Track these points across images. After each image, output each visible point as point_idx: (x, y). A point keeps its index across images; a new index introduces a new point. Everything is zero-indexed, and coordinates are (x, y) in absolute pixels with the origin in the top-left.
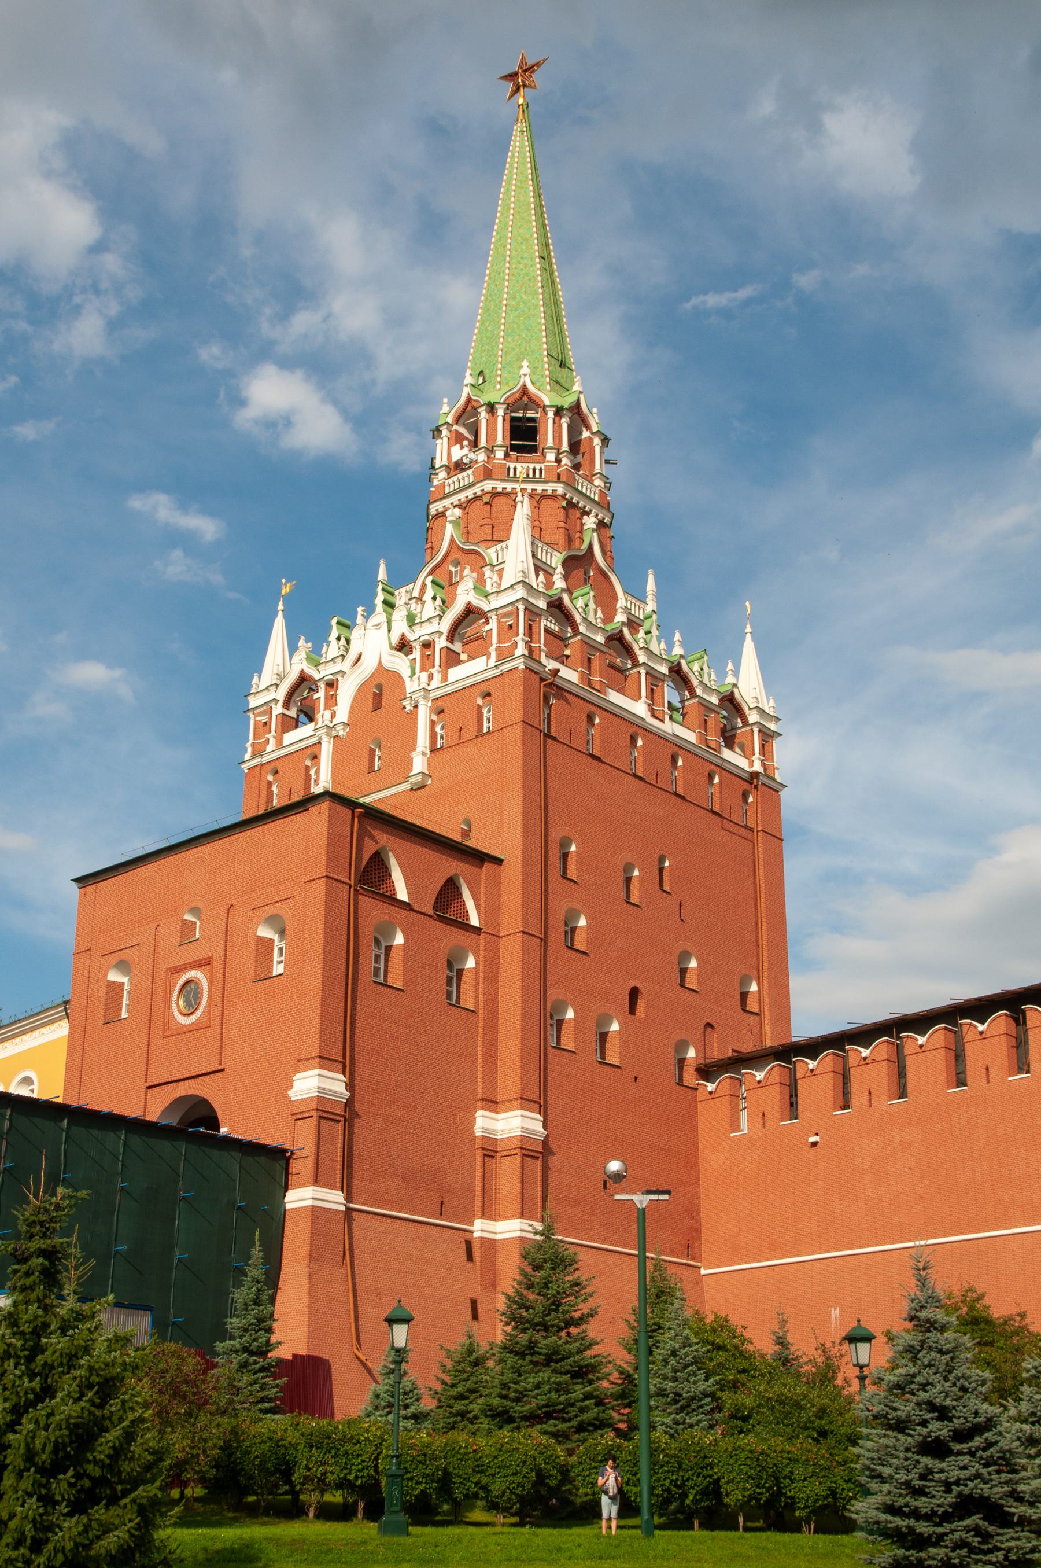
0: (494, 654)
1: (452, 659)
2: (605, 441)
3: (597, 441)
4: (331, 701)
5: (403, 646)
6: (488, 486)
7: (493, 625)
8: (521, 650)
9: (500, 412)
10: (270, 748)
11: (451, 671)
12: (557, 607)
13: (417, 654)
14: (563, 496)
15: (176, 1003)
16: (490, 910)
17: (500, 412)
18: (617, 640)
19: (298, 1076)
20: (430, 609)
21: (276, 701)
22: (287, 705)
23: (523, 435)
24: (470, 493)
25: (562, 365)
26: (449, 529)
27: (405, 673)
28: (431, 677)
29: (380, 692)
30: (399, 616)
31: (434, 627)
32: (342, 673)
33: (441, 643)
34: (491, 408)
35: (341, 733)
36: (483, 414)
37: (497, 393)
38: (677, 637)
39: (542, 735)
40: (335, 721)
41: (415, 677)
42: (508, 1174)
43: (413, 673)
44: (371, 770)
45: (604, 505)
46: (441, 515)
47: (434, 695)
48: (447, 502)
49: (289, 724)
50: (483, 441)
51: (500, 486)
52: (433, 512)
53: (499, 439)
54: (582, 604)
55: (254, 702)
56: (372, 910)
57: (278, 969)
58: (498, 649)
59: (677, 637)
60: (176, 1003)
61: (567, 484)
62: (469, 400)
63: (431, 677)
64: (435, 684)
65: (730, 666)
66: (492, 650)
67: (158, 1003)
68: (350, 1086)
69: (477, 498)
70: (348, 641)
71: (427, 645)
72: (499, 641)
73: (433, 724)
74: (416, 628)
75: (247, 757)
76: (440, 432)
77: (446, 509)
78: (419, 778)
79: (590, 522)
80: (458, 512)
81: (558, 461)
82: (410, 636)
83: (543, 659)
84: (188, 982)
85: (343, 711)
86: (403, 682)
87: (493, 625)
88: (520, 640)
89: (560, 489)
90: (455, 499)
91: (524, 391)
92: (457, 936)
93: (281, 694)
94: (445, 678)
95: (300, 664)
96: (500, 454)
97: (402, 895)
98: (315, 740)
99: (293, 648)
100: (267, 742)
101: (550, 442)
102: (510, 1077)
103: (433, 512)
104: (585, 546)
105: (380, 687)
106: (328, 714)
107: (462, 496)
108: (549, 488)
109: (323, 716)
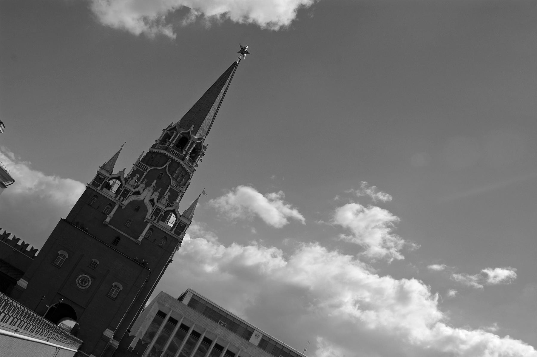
6: (181, 162)
10: (99, 188)
24: (176, 159)
26: (167, 164)
35: (123, 208)
40: (123, 203)
47: (154, 224)
50: (186, 149)
51: (183, 164)
64: (155, 222)
66: (175, 228)
71: (158, 209)
73: (149, 230)
84: (85, 277)
86: (147, 211)
94: (158, 222)
96: (188, 157)
106: (122, 198)
107: (174, 158)
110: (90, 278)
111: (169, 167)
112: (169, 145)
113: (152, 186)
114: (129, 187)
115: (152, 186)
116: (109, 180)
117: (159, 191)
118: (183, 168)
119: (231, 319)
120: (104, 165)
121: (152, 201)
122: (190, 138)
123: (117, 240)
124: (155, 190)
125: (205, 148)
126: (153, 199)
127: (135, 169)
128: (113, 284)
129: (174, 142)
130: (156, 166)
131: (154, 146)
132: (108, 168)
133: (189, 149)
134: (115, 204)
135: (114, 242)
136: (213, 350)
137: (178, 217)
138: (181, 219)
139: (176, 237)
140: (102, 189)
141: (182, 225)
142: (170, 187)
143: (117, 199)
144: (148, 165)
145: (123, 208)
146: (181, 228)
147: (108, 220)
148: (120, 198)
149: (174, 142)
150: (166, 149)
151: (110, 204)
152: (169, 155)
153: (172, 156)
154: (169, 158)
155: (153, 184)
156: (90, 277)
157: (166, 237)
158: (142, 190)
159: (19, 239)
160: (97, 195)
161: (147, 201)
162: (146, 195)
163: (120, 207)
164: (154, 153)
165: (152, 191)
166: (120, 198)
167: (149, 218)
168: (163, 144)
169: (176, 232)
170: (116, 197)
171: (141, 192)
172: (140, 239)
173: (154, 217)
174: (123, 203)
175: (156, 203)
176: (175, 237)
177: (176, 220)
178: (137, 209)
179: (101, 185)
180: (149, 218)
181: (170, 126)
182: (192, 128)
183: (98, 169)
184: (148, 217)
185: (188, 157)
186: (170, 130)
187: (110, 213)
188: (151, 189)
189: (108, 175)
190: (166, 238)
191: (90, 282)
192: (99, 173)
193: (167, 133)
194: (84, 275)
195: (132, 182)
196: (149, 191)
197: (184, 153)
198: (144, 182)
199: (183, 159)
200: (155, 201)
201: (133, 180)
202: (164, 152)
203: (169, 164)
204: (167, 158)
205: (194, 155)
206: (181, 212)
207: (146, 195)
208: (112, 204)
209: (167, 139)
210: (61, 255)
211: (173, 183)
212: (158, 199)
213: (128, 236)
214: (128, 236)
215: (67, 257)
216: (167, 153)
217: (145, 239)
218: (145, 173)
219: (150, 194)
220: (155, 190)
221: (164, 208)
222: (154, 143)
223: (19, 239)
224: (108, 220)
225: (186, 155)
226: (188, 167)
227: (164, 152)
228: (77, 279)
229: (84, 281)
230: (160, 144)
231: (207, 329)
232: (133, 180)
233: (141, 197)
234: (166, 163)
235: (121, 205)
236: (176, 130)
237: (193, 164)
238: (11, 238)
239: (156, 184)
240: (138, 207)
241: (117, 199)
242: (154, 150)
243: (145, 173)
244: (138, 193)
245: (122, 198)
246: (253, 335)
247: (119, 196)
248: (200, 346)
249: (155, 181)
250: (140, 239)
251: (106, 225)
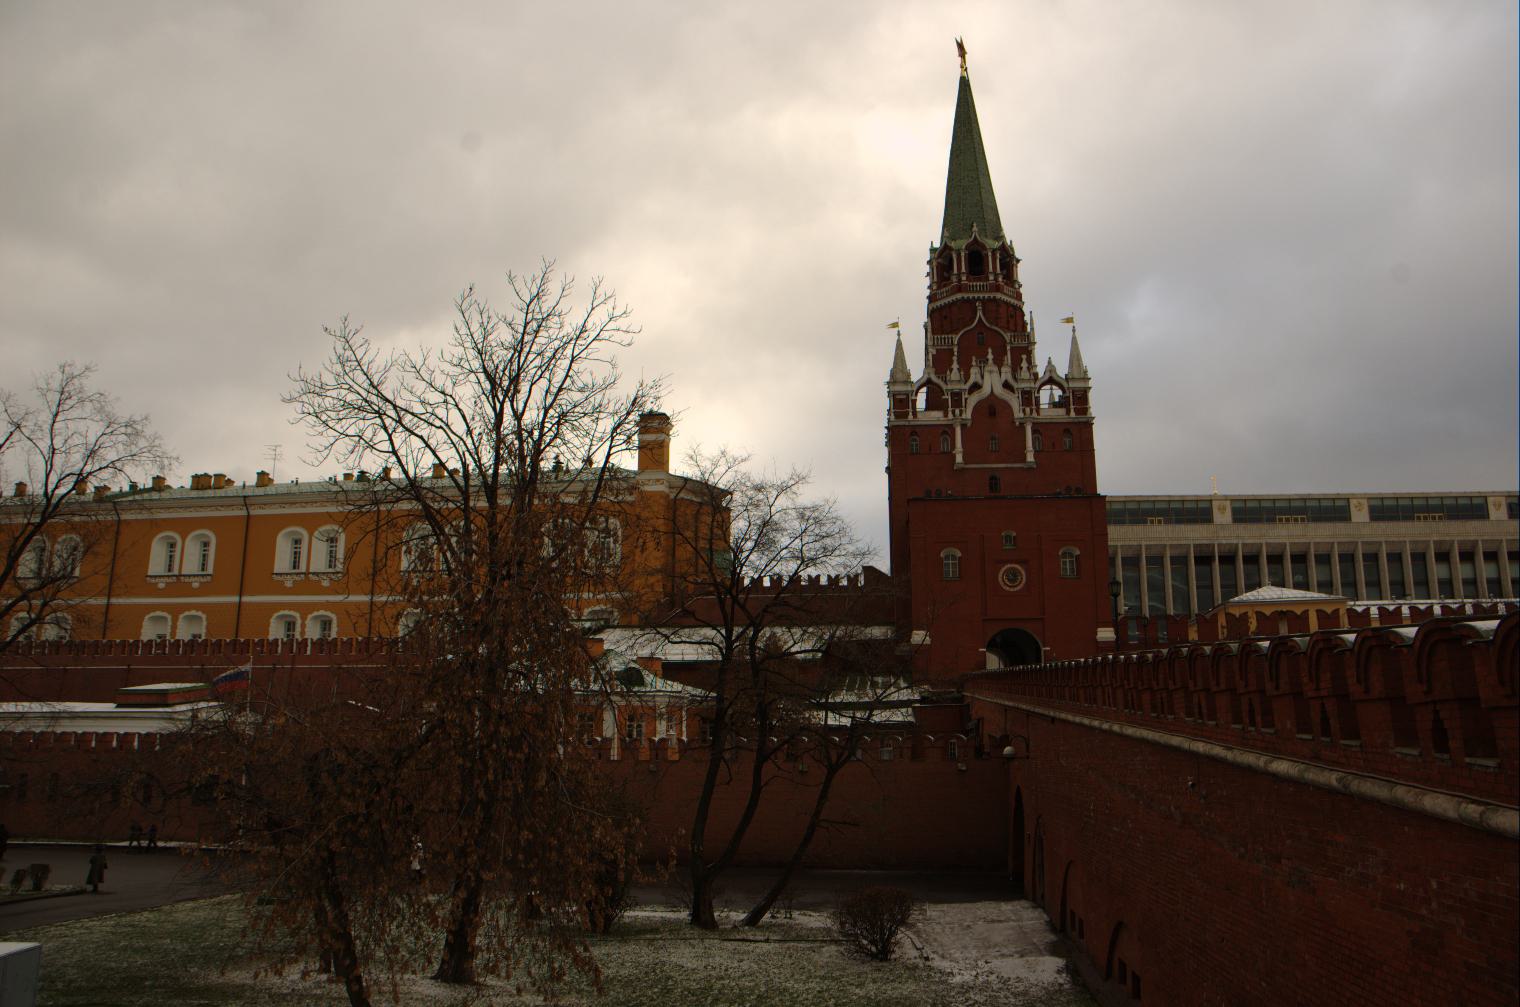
0: (1072, 411)
6: (999, 296)
10: (911, 417)
19: (1099, 629)
24: (986, 296)
26: (980, 313)
28: (1031, 411)
34: (994, 252)
35: (969, 425)
40: (964, 416)
53: (998, 271)
66: (1072, 407)
94: (1038, 414)
96: (1000, 279)
100: (907, 414)
106: (957, 411)
107: (981, 296)
110: (1017, 566)
111: (984, 314)
112: (960, 280)
113: (990, 361)
114: (957, 387)
115: (990, 361)
116: (916, 395)
117: (1006, 362)
118: (1007, 304)
119: (1164, 506)
120: (892, 375)
121: (1006, 385)
122: (983, 247)
123: (993, 481)
124: (999, 362)
125: (1012, 249)
126: (1006, 381)
127: (933, 351)
128: (1060, 553)
129: (963, 270)
130: (964, 327)
131: (931, 299)
132: (900, 376)
133: (993, 265)
134: (951, 428)
135: (991, 488)
136: (1173, 570)
137: (1065, 385)
138: (1071, 385)
139: (1084, 420)
141: (1079, 395)
142: (1008, 348)
143: (950, 416)
144: (951, 332)
145: (969, 425)
146: (1076, 397)
147: (959, 459)
148: (953, 412)
149: (963, 270)
150: (959, 289)
151: (945, 432)
152: (971, 296)
153: (976, 296)
154: (975, 300)
155: (990, 356)
156: (1016, 563)
157: (1066, 428)
158: (979, 376)
159: (818, 577)
160: (915, 430)
161: (999, 391)
162: (992, 381)
163: (963, 426)
164: (942, 308)
165: (996, 369)
166: (953, 412)
167: (1022, 415)
168: (945, 286)
169: (1077, 412)
170: (946, 415)
171: (980, 381)
172: (1030, 458)
173: (1028, 410)
174: (964, 416)
175: (1015, 385)
176: (1081, 420)
177: (1064, 392)
178: (992, 413)
179: (910, 410)
180: (1022, 415)
181: (933, 250)
182: (975, 229)
183: (885, 390)
184: (1018, 414)
185: (1000, 279)
186: (939, 256)
187: (953, 446)
188: (991, 366)
189: (909, 388)
190: (1067, 431)
191: (1023, 573)
192: (892, 395)
193: (938, 263)
194: (1004, 569)
195: (955, 375)
196: (991, 372)
197: (991, 277)
198: (974, 363)
199: (998, 289)
200: (1011, 381)
201: (955, 370)
202: (959, 296)
204: (971, 302)
205: (1005, 272)
206: (1062, 370)
207: (992, 381)
208: (947, 431)
209: (946, 274)
210: (947, 557)
211: (1007, 336)
213: (1009, 465)
214: (1009, 465)
215: (959, 554)
216: (966, 296)
217: (1037, 453)
218: (956, 349)
219: (996, 375)
220: (999, 362)
221: (1032, 385)
222: (928, 292)
223: (818, 577)
224: (959, 459)
225: (996, 279)
226: (1010, 296)
227: (959, 296)
228: (1000, 579)
229: (1013, 576)
230: (939, 288)
231: (1144, 543)
232: (955, 370)
233: (986, 390)
234: (976, 314)
235: (964, 422)
236: (951, 249)
237: (1013, 287)
238: (823, 581)
239: (993, 353)
240: (992, 408)
241: (950, 416)
242: (938, 304)
243: (956, 349)
244: (976, 387)
245: (957, 411)
246: (1215, 511)
247: (950, 409)
248: (1148, 577)
249: (990, 351)
250: (1030, 458)
251: (963, 469)
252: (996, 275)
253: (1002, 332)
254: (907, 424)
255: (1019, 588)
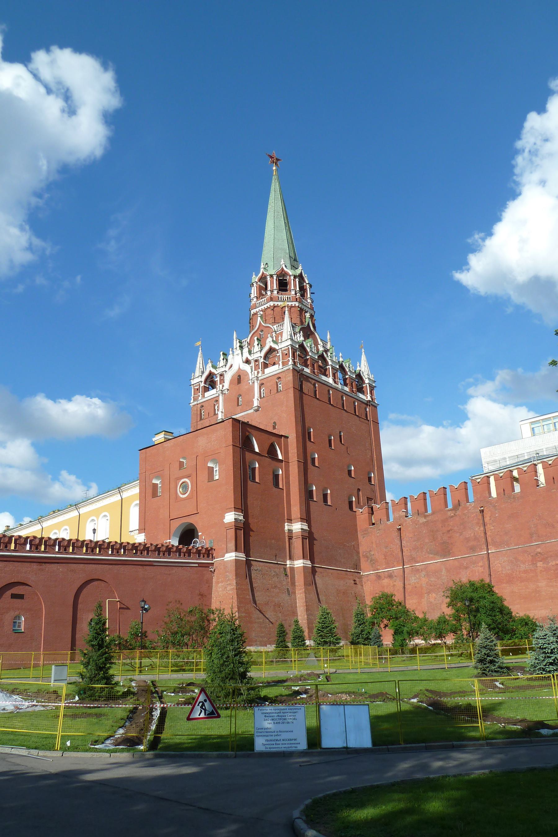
1: (266, 366)
2: (311, 286)
3: (308, 286)
4: (222, 381)
5: (247, 362)
6: (272, 303)
7: (280, 354)
8: (291, 362)
9: (275, 278)
10: (200, 398)
11: (266, 370)
12: (302, 346)
13: (253, 364)
14: (298, 307)
15: (179, 490)
16: (286, 453)
17: (275, 278)
18: (322, 357)
19: (227, 514)
20: (256, 348)
21: (201, 382)
22: (205, 383)
23: (283, 286)
24: (265, 306)
25: (295, 260)
27: (249, 371)
28: (258, 373)
29: (239, 378)
30: (246, 350)
31: (258, 355)
32: (226, 371)
33: (262, 360)
34: (271, 276)
36: (269, 278)
37: (272, 271)
38: (341, 355)
39: (299, 391)
40: (224, 388)
41: (253, 373)
42: (297, 544)
43: (252, 371)
44: (238, 405)
45: (312, 309)
46: (256, 314)
48: (257, 310)
49: (206, 389)
50: (269, 288)
51: (276, 303)
52: (252, 313)
53: (275, 287)
54: (308, 344)
55: (193, 382)
56: (248, 455)
57: (217, 477)
58: (283, 362)
59: (341, 355)
60: (179, 490)
61: (299, 302)
62: (263, 273)
63: (258, 373)
64: (260, 375)
65: (358, 364)
66: (280, 363)
67: (172, 491)
68: (309, 526)
69: (268, 308)
70: (227, 360)
71: (256, 361)
72: (283, 359)
74: (252, 355)
75: (192, 401)
76: (253, 285)
77: (257, 312)
78: (257, 408)
79: (308, 315)
80: (261, 313)
81: (296, 294)
82: (250, 358)
83: (299, 366)
85: (226, 385)
87: (280, 354)
88: (290, 359)
89: (297, 304)
90: (260, 308)
91: (283, 269)
92: (274, 463)
93: (203, 379)
95: (209, 368)
96: (275, 292)
97: (257, 450)
98: (217, 395)
99: (206, 363)
101: (292, 288)
102: (296, 510)
103: (252, 313)
104: (306, 324)
105: (239, 376)
106: (221, 386)
107: (263, 307)
108: (293, 304)
109: (219, 386)
129: (256, 295)
140: (204, 396)
156: (188, 477)
172: (256, 403)
197: (269, 293)
199: (271, 299)
203: (261, 317)
212: (250, 352)
235: (224, 392)
247: (218, 387)
252: (272, 291)
253: (271, 326)
254: (198, 402)
255: (186, 495)
